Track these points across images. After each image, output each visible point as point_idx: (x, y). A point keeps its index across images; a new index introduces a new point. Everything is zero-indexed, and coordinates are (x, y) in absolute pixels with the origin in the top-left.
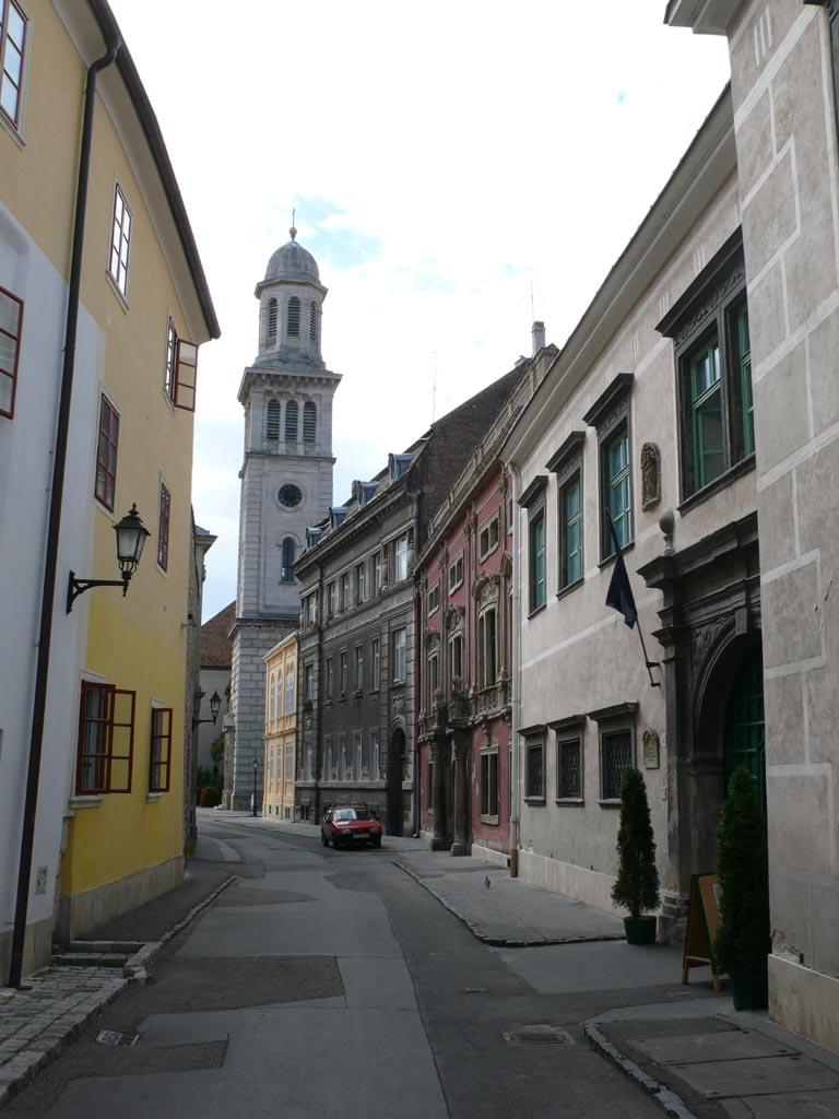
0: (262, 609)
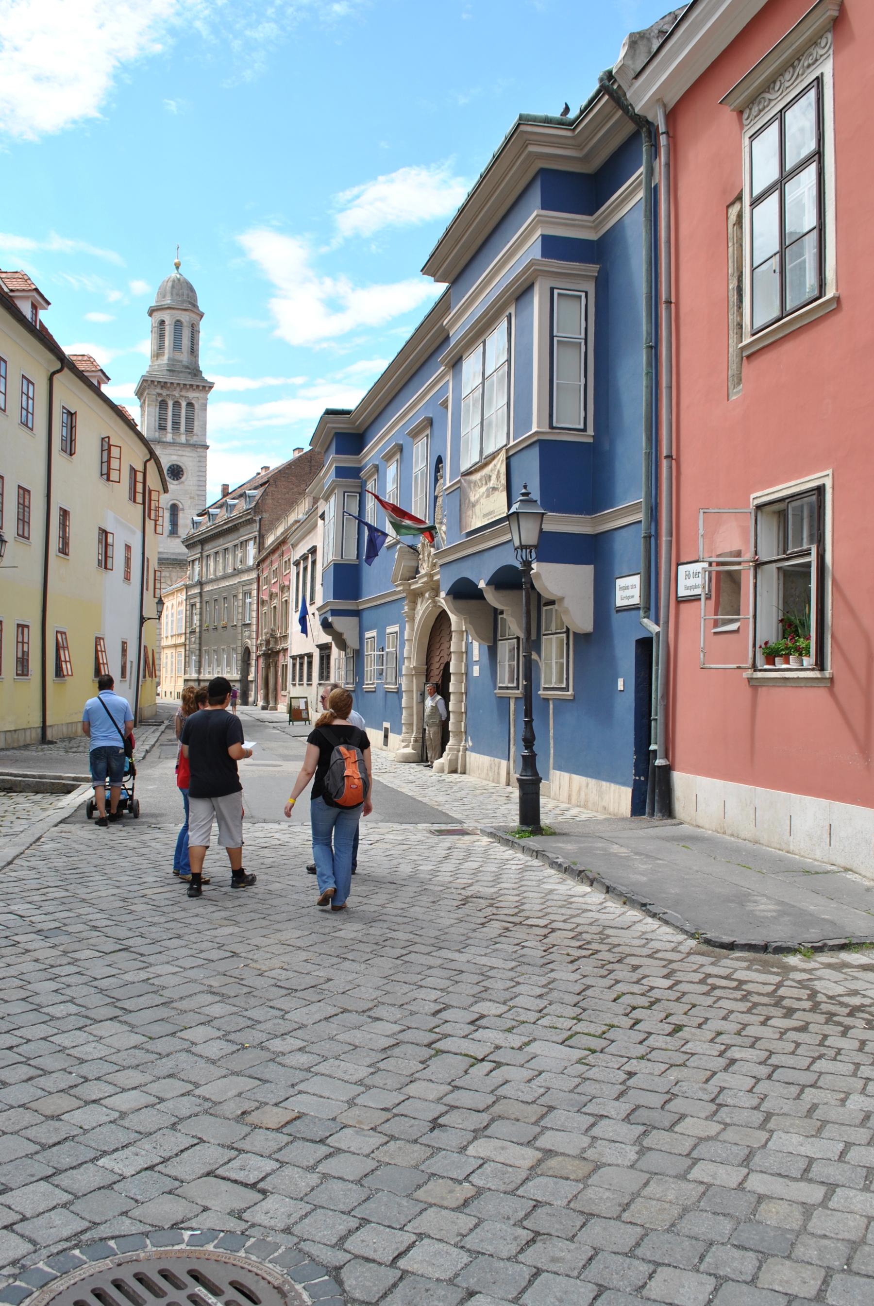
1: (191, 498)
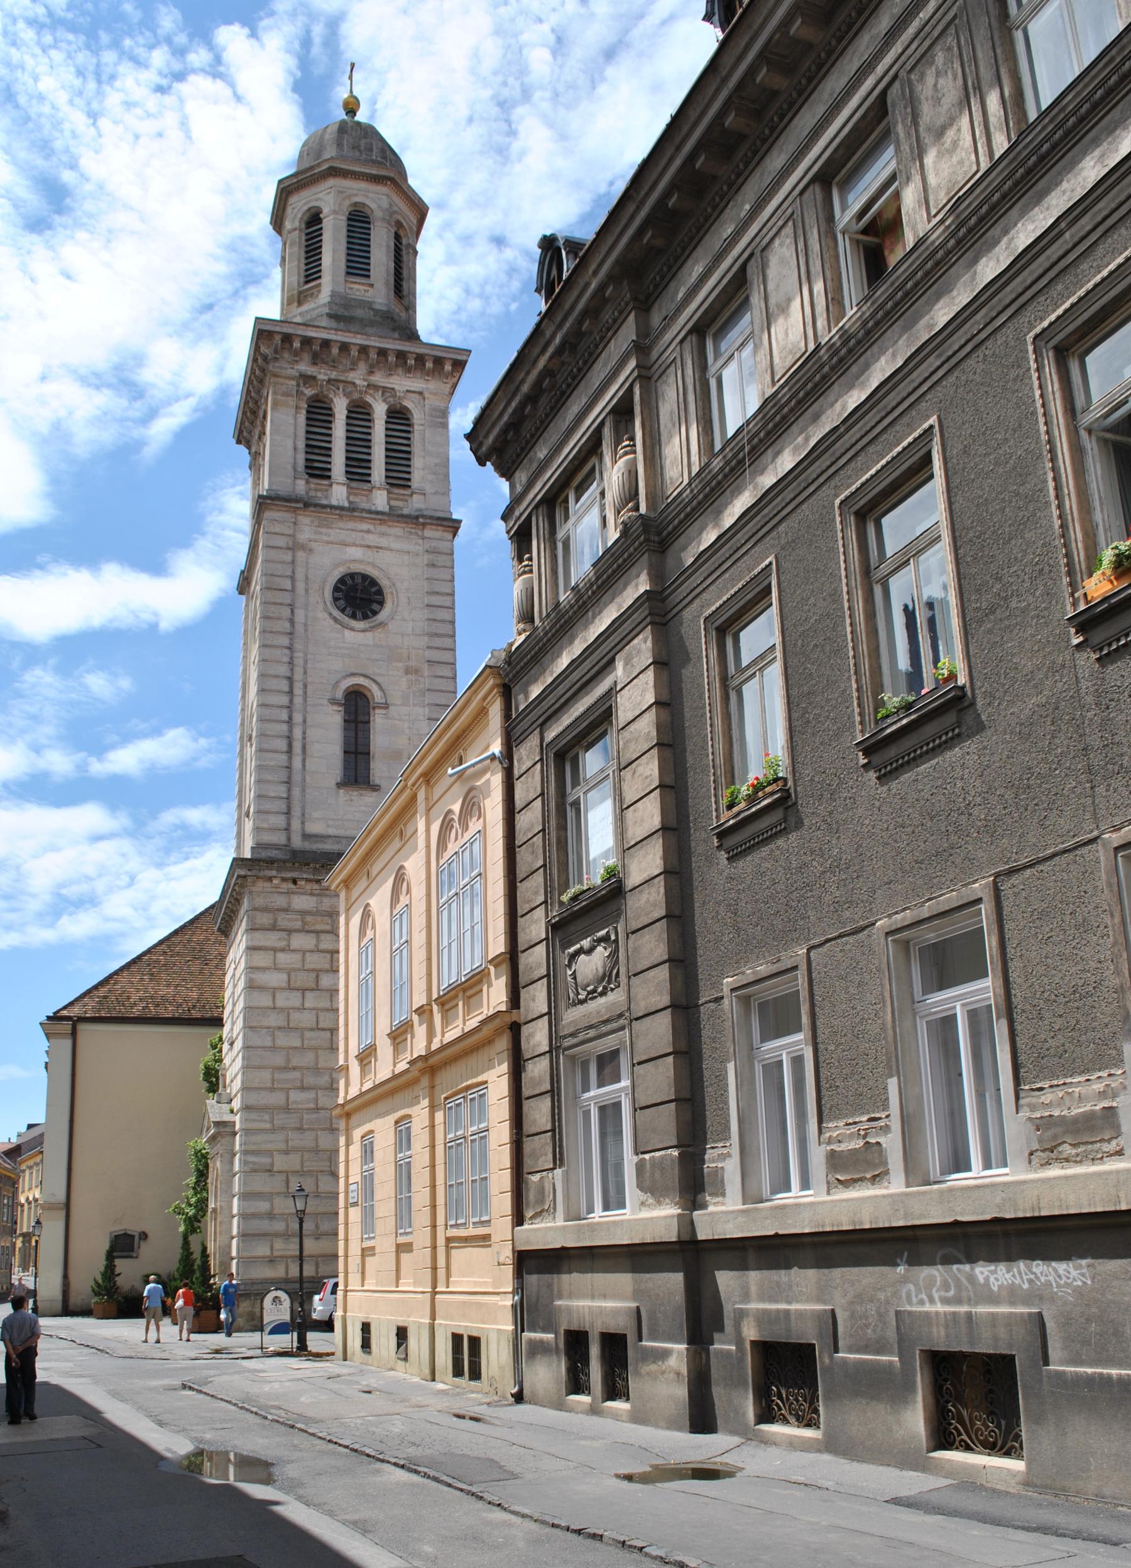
0: (297, 842)
1: (408, 671)
